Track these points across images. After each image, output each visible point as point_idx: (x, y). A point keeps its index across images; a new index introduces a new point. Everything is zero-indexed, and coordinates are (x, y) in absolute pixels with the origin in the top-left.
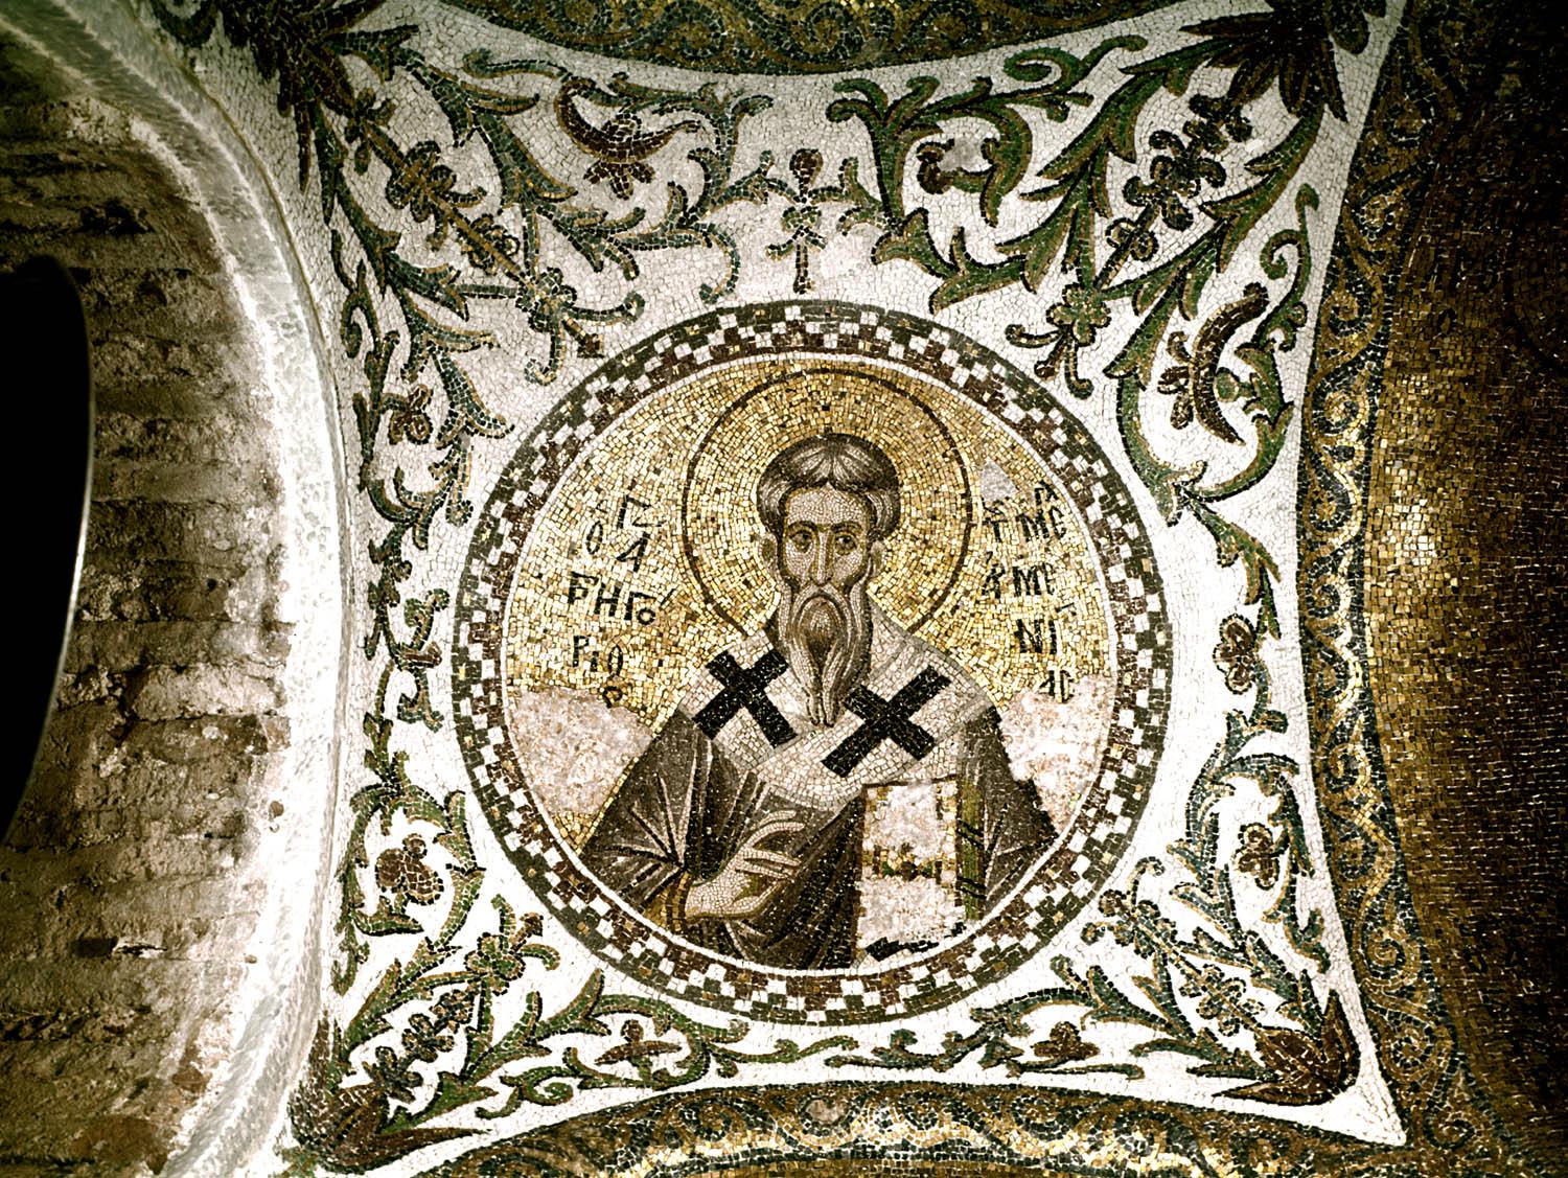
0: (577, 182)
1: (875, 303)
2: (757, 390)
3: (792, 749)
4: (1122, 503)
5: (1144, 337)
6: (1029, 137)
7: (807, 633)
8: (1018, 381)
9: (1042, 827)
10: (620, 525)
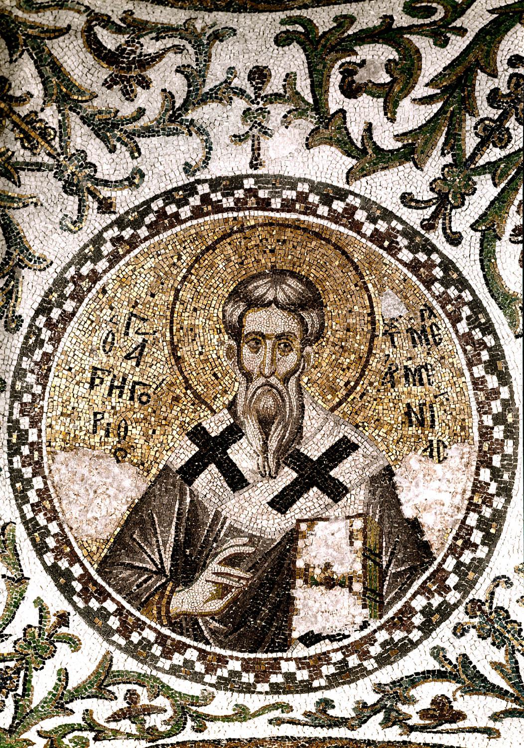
0: (97, 88)
1: (308, 177)
2: (223, 238)
3: (246, 493)
4: (483, 321)
6: (420, 59)
7: (258, 412)
9: (423, 552)
10: (127, 334)
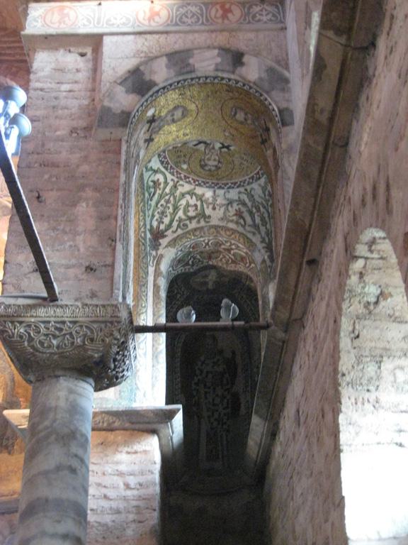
5: (165, 188)
8: (181, 179)
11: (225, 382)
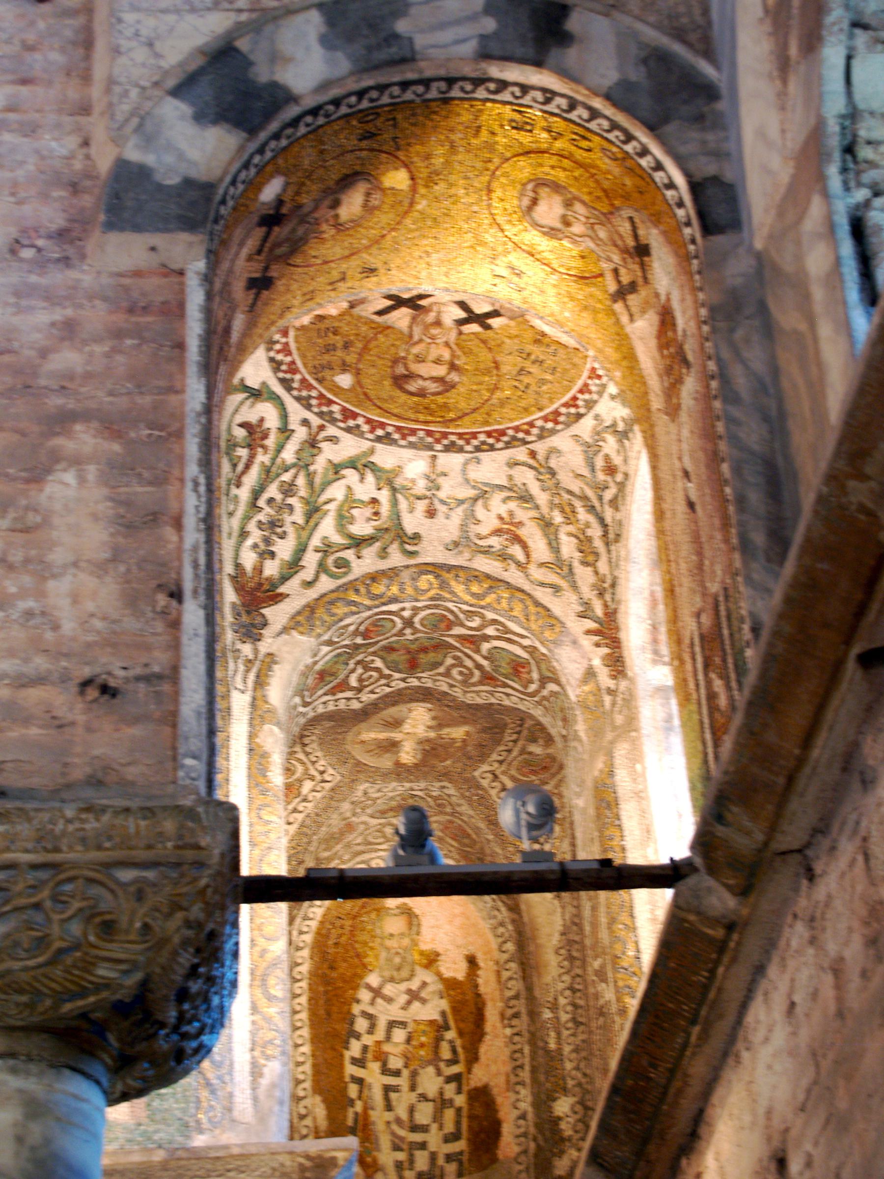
5: (280, 448)
8: (333, 421)
11: (446, 1054)
